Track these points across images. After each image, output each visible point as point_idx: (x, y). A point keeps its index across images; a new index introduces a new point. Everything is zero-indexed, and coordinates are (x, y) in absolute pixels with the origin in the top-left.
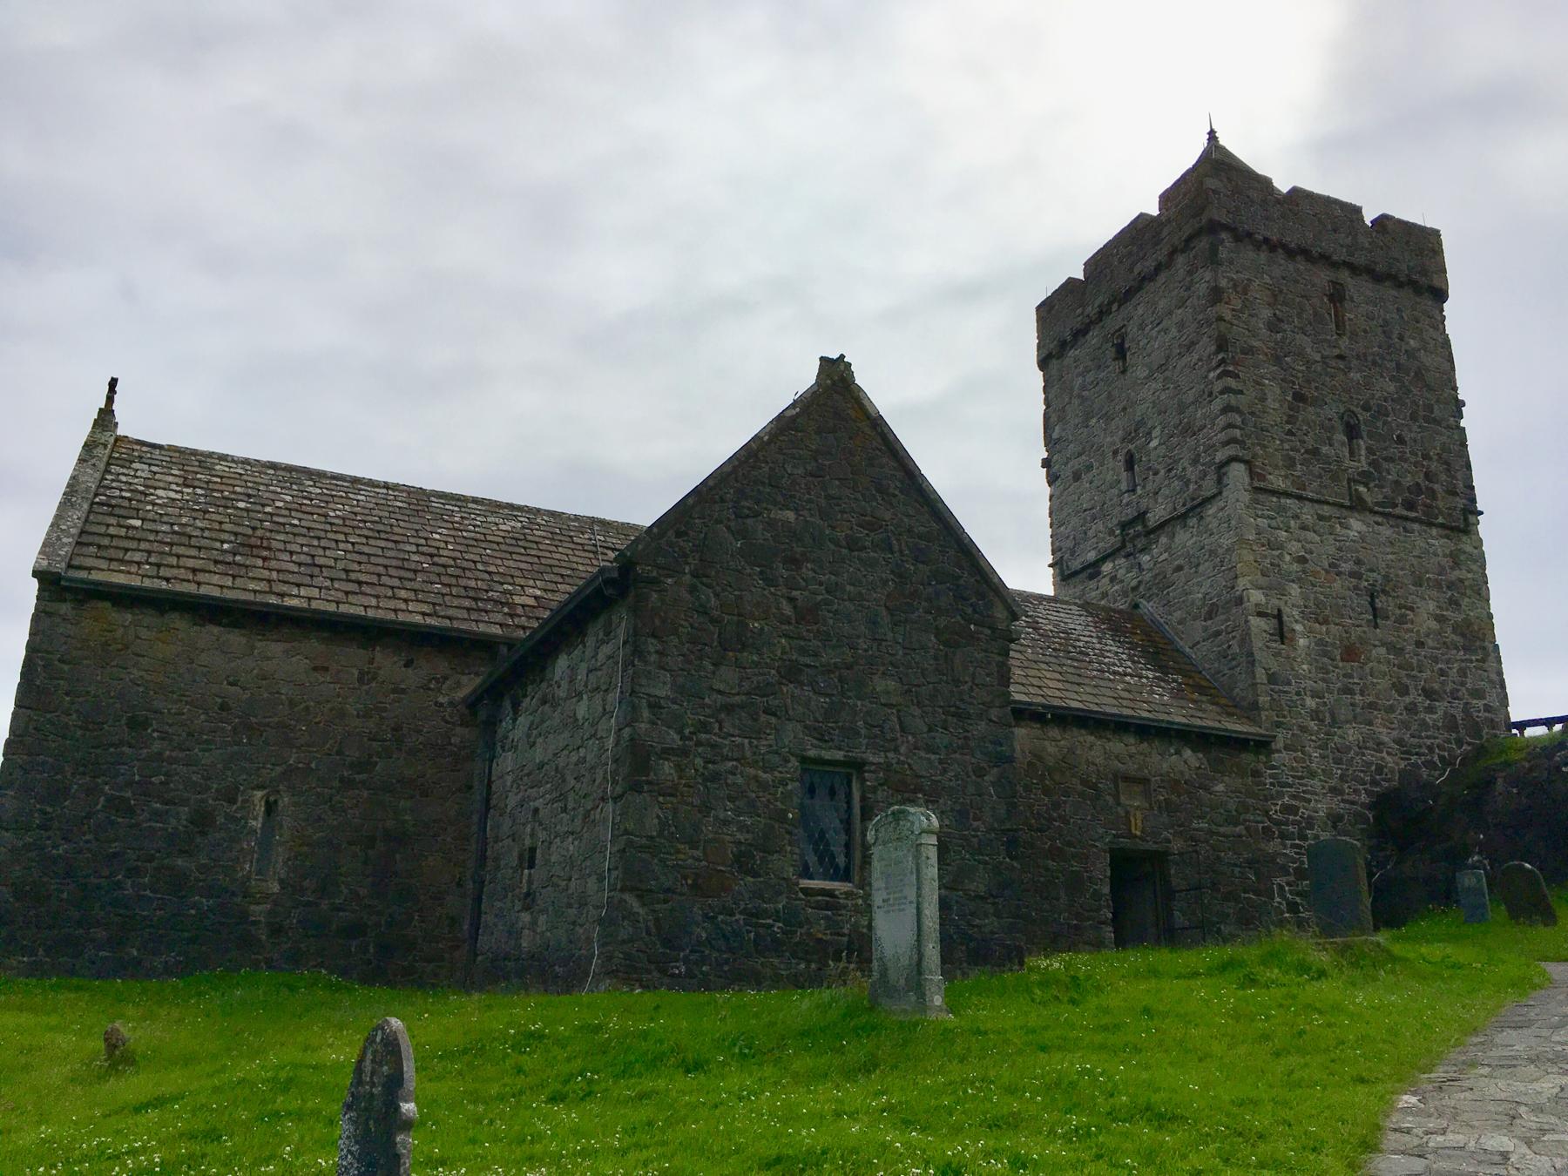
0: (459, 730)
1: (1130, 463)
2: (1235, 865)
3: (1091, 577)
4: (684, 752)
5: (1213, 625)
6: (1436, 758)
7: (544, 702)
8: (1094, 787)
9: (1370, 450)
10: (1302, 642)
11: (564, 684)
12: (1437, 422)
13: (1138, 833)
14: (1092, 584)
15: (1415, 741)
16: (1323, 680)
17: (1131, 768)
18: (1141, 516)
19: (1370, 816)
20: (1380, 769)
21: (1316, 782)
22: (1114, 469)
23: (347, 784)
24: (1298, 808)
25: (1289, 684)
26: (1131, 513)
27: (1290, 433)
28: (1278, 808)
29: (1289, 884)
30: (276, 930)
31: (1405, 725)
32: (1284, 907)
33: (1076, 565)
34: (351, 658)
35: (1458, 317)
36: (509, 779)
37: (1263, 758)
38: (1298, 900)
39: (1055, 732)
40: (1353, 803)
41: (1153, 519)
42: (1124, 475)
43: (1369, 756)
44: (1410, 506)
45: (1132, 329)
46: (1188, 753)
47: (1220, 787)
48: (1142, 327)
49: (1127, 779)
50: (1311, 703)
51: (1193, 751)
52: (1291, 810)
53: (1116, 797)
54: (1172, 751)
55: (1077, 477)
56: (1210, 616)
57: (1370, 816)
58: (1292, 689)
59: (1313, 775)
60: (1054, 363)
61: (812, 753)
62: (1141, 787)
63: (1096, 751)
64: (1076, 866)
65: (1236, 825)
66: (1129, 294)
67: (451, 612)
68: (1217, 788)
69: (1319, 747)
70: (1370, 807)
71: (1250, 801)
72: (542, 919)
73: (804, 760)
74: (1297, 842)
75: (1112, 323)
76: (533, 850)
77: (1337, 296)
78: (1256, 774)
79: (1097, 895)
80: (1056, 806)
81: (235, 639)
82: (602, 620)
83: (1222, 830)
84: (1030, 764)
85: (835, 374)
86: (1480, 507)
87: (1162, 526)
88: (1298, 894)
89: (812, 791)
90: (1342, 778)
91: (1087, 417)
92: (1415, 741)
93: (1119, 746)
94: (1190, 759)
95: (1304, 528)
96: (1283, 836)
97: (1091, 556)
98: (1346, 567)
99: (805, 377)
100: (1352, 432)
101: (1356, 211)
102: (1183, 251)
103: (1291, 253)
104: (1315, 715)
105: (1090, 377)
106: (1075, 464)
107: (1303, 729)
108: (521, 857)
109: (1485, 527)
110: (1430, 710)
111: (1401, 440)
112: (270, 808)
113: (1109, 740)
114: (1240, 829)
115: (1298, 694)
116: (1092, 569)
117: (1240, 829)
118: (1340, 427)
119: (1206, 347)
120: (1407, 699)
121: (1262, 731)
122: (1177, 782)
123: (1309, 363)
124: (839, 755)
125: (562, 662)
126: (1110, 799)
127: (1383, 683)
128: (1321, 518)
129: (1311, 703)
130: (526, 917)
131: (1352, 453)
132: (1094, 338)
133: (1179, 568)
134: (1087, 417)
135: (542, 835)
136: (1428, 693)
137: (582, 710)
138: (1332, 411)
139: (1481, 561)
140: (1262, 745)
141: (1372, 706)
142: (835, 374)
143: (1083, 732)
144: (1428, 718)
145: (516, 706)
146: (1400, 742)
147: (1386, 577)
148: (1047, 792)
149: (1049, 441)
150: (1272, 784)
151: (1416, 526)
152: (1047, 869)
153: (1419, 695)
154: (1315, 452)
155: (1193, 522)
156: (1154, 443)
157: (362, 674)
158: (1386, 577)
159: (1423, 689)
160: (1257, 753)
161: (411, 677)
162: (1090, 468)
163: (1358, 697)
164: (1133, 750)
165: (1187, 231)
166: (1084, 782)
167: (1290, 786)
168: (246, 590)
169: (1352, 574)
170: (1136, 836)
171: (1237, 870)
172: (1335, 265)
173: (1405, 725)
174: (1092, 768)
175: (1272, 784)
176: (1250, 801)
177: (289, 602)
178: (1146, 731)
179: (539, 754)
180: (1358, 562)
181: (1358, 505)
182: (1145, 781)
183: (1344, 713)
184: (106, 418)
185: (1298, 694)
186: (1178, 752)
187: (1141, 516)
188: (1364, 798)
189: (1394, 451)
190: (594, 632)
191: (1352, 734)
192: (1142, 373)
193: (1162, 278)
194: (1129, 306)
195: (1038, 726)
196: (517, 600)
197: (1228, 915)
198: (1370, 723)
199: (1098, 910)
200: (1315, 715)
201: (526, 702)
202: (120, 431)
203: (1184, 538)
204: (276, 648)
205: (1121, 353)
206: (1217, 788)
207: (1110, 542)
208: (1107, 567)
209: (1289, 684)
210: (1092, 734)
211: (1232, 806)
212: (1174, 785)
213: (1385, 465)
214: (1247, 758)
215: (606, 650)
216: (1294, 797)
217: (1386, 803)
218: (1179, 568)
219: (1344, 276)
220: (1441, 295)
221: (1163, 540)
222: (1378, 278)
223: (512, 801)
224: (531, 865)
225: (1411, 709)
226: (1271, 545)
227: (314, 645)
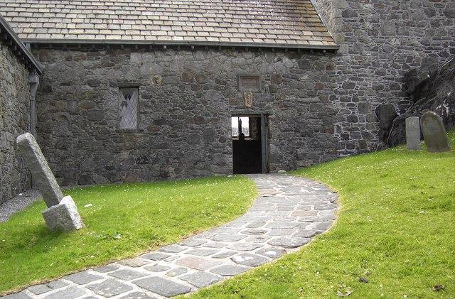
2: (311, 118)
6: (448, 51)
8: (225, 83)
13: (249, 106)
15: (433, 42)
16: (378, 12)
17: (248, 71)
19: (401, 85)
20: (410, 59)
21: (367, 70)
24: (354, 84)
25: (356, 16)
28: (341, 85)
29: (343, 125)
31: (431, 33)
32: (339, 137)
37: (335, 59)
38: (349, 133)
40: (389, 79)
43: (404, 52)
46: (286, 60)
47: (306, 77)
49: (244, 77)
50: (369, 25)
51: (291, 58)
53: (237, 87)
54: (276, 59)
57: (401, 85)
58: (358, 19)
59: (366, 66)
62: (254, 81)
63: (225, 64)
64: (210, 125)
68: (302, 78)
69: (371, 50)
70: (402, 80)
71: (324, 83)
74: (352, 102)
78: (329, 67)
80: (199, 96)
83: (304, 100)
84: (185, 74)
88: (349, 130)
90: (385, 66)
92: (433, 42)
93: (240, 59)
94: (287, 62)
96: (342, 100)
104: (373, 33)
107: (362, 41)
110: (448, 23)
113: (236, 57)
114: (317, 99)
115: (362, 21)
117: (317, 99)
120: (433, 18)
121: (333, 44)
122: (278, 76)
126: (233, 89)
127: (421, 10)
129: (369, 25)
140: (332, 52)
141: (408, 24)
143: (218, 54)
144: (446, 28)
146: (425, 43)
148: (194, 88)
150: (338, 73)
152: (192, 128)
153: (442, 15)
159: (445, 12)
160: (331, 57)
163: (401, 20)
164: (251, 61)
166: (218, 81)
167: (350, 73)
170: (247, 107)
171: (311, 120)
173: (431, 33)
174: (225, 73)
175: (338, 73)
176: (324, 83)
178: (256, 50)
182: (257, 78)
183: (390, 29)
185: (362, 21)
186: (280, 60)
188: (398, 76)
191: (395, 42)
195: (190, 53)
197: (304, 144)
198: (407, 34)
199: (224, 147)
200: (373, 33)
206: (302, 78)
209: (356, 16)
210: (225, 54)
211: (312, 86)
212: (276, 78)
216: (353, 79)
217: (408, 77)
225: (435, 24)
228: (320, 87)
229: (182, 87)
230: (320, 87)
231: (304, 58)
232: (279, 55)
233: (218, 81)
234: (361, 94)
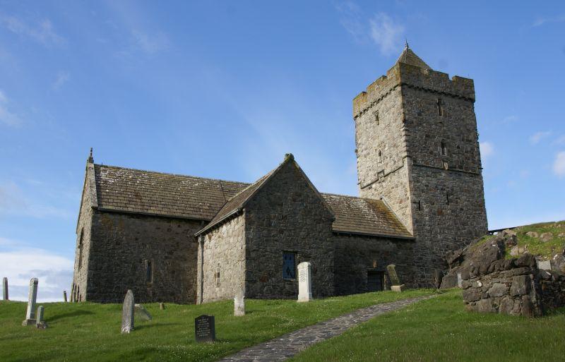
0: (193, 243)
1: (380, 154)
3: (370, 188)
4: (258, 251)
5: (402, 205)
7: (219, 237)
9: (449, 151)
10: (426, 210)
11: (226, 234)
12: (470, 141)
14: (370, 191)
18: (383, 171)
22: (374, 155)
23: (166, 258)
26: (380, 170)
27: (424, 147)
30: (154, 294)
33: (365, 185)
34: (165, 224)
35: (478, 107)
36: (209, 256)
37: (413, 244)
39: (352, 239)
41: (386, 173)
42: (379, 158)
44: (461, 167)
45: (380, 112)
46: (391, 244)
47: (400, 253)
49: (373, 252)
52: (421, 259)
53: (369, 256)
55: (365, 157)
56: (401, 202)
61: (285, 250)
62: (377, 254)
63: (364, 244)
65: (404, 263)
67: (188, 212)
72: (223, 289)
73: (284, 252)
75: (375, 108)
76: (219, 274)
78: (411, 249)
79: (364, 284)
81: (137, 221)
82: (236, 219)
85: (290, 159)
86: (482, 166)
87: (387, 175)
89: (286, 258)
91: (368, 137)
95: (428, 176)
97: (370, 182)
98: (440, 187)
99: (282, 160)
100: (443, 145)
101: (447, 75)
102: (394, 90)
103: (426, 91)
105: (369, 124)
106: (365, 152)
108: (215, 275)
109: (484, 173)
111: (458, 147)
112: (149, 264)
114: (405, 265)
116: (369, 186)
117: (405, 265)
118: (440, 144)
122: (388, 252)
123: (431, 125)
124: (292, 250)
125: (224, 227)
128: (433, 172)
130: (217, 289)
131: (443, 153)
132: (370, 112)
133: (393, 188)
134: (368, 137)
135: (221, 270)
136: (464, 224)
137: (231, 240)
138: (438, 139)
142: (290, 159)
145: (210, 238)
147: (452, 190)
148: (350, 255)
149: (357, 143)
151: (462, 174)
154: (431, 153)
155: (396, 174)
156: (386, 149)
157: (168, 230)
158: (452, 190)
161: (180, 230)
162: (368, 154)
165: (395, 84)
168: (138, 209)
169: (442, 189)
172: (440, 94)
177: (149, 212)
178: (378, 238)
179: (218, 250)
180: (445, 186)
182: (378, 252)
184: (91, 160)
187: (383, 171)
189: (456, 151)
190: (233, 222)
192: (383, 126)
193: (388, 96)
194: (379, 104)
196: (204, 207)
200: (430, 231)
201: (213, 237)
202: (95, 163)
203: (394, 178)
204: (148, 224)
205: (377, 118)
207: (374, 178)
208: (374, 186)
213: (454, 155)
214: (408, 244)
215: (237, 227)
218: (393, 188)
219: (442, 96)
220: (473, 101)
221: (389, 179)
222: (453, 97)
223: (211, 262)
224: (219, 276)
226: (418, 182)
227: (156, 222)
228: (407, 259)
229: (345, 255)
230: (407, 259)
231: (399, 243)
232: (388, 241)
233: (361, 253)
234: (426, 263)
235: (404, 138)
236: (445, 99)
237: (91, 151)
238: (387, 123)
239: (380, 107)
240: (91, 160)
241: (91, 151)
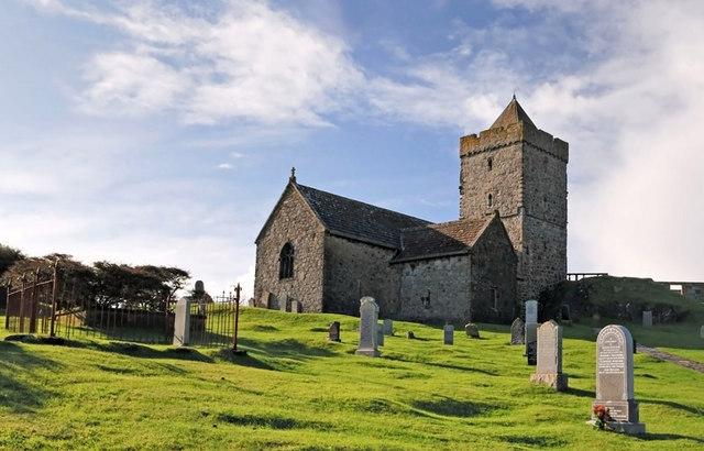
1: (490, 197)
48: (498, 160)
60: (466, 160)
66: (495, 149)
75: (489, 155)
77: (546, 162)
100: (545, 200)
108: (423, 299)
119: (518, 173)
125: (438, 262)
132: (481, 156)
139: (566, 235)
145: (413, 267)
179: (428, 278)
181: (544, 220)
184: (293, 180)
215: (458, 264)
235: (521, 190)
236: (551, 158)
237: (293, 170)
238: (502, 171)
239: (496, 155)
240: (293, 180)
241: (293, 170)
